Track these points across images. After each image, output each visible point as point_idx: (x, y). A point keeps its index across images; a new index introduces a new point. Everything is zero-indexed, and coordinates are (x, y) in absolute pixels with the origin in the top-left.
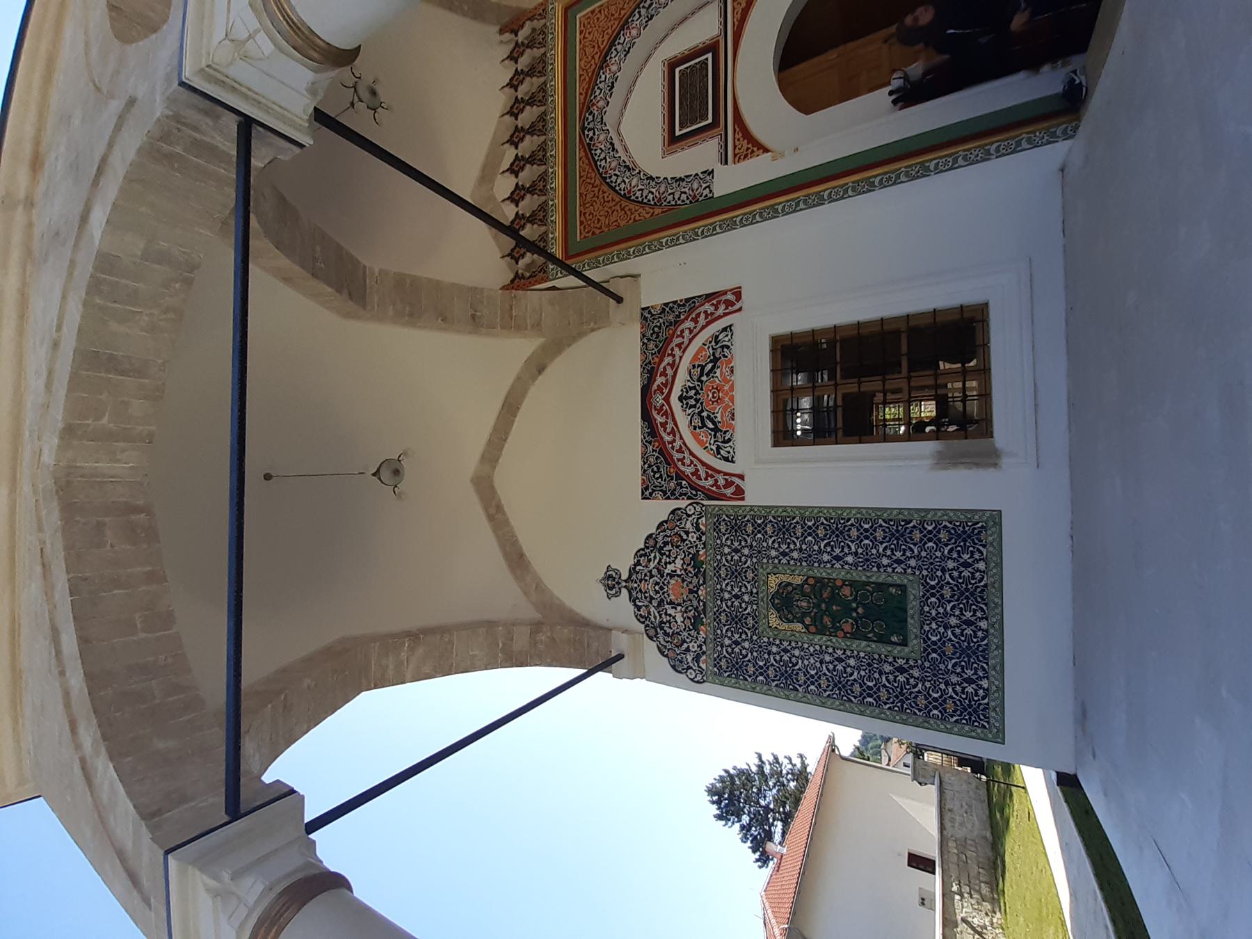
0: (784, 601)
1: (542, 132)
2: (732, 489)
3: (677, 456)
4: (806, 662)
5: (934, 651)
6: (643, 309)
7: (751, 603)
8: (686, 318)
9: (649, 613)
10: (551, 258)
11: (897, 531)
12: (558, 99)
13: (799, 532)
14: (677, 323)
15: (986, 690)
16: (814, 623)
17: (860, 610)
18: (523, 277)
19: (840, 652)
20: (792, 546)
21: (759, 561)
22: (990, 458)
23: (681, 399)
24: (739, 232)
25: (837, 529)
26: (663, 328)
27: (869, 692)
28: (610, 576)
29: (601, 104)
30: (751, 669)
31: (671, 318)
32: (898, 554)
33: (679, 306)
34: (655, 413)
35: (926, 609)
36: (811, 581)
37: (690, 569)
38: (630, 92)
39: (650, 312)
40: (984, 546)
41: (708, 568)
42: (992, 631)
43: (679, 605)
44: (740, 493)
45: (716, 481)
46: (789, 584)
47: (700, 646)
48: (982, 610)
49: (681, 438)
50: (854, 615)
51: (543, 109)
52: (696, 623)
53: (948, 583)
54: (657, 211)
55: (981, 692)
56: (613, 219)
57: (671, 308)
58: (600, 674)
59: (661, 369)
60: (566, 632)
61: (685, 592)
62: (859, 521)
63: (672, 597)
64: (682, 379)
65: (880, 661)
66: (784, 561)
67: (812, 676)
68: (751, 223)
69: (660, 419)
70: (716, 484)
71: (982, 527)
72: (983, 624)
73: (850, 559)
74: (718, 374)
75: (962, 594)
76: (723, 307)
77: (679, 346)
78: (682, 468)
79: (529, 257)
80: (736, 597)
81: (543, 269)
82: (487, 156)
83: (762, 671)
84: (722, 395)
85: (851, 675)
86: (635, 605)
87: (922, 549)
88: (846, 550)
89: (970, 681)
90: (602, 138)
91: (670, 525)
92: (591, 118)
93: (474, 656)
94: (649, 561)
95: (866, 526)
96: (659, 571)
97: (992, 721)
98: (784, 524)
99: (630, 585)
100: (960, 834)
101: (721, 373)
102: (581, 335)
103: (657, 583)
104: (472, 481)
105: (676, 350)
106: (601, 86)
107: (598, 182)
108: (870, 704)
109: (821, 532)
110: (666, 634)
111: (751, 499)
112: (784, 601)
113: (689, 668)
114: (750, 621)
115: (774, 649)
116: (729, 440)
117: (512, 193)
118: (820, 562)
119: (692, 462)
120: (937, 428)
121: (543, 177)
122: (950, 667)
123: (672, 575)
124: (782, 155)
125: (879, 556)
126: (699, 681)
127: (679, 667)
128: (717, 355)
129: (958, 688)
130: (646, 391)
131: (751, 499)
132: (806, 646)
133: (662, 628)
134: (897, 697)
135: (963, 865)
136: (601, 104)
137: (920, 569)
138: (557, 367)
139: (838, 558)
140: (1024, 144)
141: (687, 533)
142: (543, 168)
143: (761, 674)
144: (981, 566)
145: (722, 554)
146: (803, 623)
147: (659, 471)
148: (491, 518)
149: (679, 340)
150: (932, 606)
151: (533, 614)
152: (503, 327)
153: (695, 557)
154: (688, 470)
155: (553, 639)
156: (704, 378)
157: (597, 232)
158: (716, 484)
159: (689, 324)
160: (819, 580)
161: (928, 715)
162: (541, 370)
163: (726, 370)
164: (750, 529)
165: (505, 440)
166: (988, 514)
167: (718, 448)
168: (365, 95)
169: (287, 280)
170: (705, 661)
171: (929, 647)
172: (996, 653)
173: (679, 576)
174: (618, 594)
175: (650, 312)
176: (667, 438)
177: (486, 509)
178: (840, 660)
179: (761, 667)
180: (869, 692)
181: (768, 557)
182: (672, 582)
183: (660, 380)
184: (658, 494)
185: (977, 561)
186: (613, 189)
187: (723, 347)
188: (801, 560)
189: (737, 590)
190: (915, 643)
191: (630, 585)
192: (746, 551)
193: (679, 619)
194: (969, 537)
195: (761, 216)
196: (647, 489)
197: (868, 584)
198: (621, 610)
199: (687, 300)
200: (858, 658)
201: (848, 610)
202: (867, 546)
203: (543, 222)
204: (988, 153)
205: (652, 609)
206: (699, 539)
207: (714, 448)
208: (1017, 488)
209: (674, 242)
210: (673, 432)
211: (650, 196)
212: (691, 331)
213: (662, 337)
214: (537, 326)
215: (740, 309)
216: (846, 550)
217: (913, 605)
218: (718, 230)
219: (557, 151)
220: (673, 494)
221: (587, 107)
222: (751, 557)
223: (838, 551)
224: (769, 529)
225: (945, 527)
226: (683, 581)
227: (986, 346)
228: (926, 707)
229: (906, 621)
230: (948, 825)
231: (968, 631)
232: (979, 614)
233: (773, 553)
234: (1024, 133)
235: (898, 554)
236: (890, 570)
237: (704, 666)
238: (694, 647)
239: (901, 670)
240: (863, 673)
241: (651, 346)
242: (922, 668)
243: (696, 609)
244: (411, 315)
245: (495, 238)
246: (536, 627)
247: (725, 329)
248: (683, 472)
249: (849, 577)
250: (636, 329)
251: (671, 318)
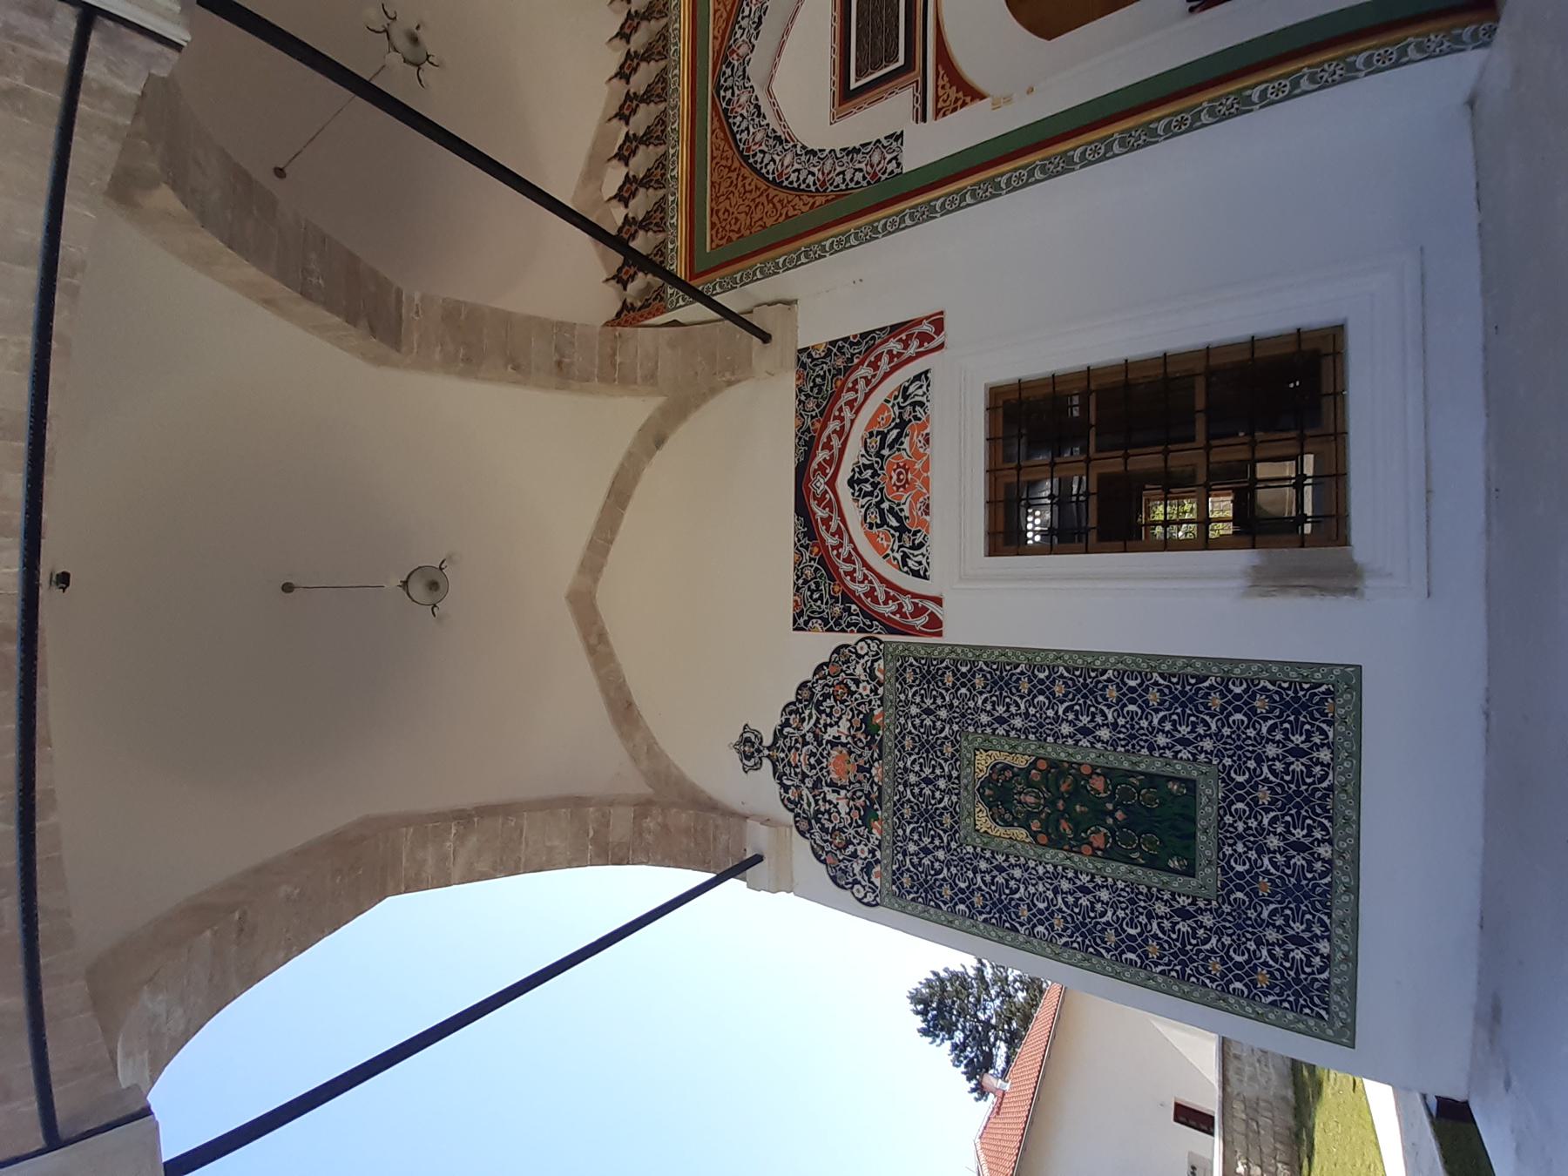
0: (1000, 792)
1: (662, 98)
2: (924, 619)
3: (845, 568)
4: (1032, 890)
5: (1240, 888)
6: (800, 351)
7: (950, 792)
8: (861, 363)
9: (801, 797)
10: (671, 278)
11: (1184, 693)
12: (684, 47)
13: (1025, 687)
14: (849, 369)
15: (1327, 959)
16: (1045, 825)
17: (1119, 815)
18: (633, 308)
19: (1085, 878)
20: (1013, 709)
21: (962, 730)
22: (1345, 580)
23: (851, 483)
24: (940, 222)
25: (1085, 685)
26: (828, 377)
27: (1131, 944)
28: (748, 740)
29: (742, 51)
30: (947, 892)
31: (840, 363)
32: (1184, 730)
33: (852, 344)
34: (814, 504)
35: (1228, 819)
36: (1042, 765)
37: (860, 735)
38: (787, 32)
39: (810, 356)
40: (1330, 723)
41: (887, 736)
42: (1339, 863)
43: (843, 787)
44: (935, 624)
45: (901, 606)
46: (1007, 767)
47: (872, 852)
48: (1324, 828)
49: (851, 541)
50: (1110, 821)
51: (662, 64)
52: (867, 816)
53: (1266, 780)
54: (820, 200)
55: (1317, 960)
56: (756, 217)
57: (840, 349)
58: (732, 880)
59: (824, 439)
60: (684, 818)
61: (852, 768)
62: (1121, 674)
63: (834, 776)
64: (854, 453)
65: (1149, 896)
66: (1001, 731)
67: (1041, 912)
68: (959, 208)
69: (820, 513)
71: (1328, 692)
72: (1324, 851)
73: (1104, 733)
74: (906, 446)
75: (1290, 799)
76: (916, 343)
77: (850, 403)
78: (852, 586)
79: (641, 280)
80: (927, 781)
81: (659, 295)
82: (594, 144)
83: (964, 896)
84: (913, 477)
85: (1103, 914)
86: (782, 784)
87: (1224, 722)
88: (1099, 719)
89: (1298, 941)
90: (743, 99)
91: (832, 669)
92: (729, 71)
93: (551, 849)
94: (803, 720)
95: (1132, 683)
96: (816, 737)
97: (1334, 1007)
98: (1002, 674)
99: (774, 753)
100: (1249, 1091)
101: (911, 444)
102: (714, 391)
103: (813, 754)
104: (567, 597)
105: (847, 410)
106: (744, 23)
107: (736, 164)
108: (1131, 963)
109: (1059, 689)
110: (824, 829)
111: (954, 633)
112: (1000, 792)
113: (856, 882)
114: (947, 820)
115: (983, 865)
116: (921, 545)
117: (621, 189)
118: (1056, 736)
119: (866, 577)
120: (1252, 527)
121: (662, 163)
122: (1265, 915)
123: (834, 743)
124: (1008, 100)
125: (1152, 731)
126: (870, 903)
127: (841, 879)
128: (906, 417)
129: (1278, 951)
130: (802, 472)
131: (954, 633)
132: (1032, 864)
133: (818, 821)
134: (1175, 955)
135: (1252, 1137)
136: (742, 51)
137: (1220, 755)
138: (681, 439)
139: (1085, 731)
140: (1412, 53)
141: (857, 682)
142: (661, 149)
143: (962, 901)
144: (1325, 755)
145: (907, 716)
146: (1028, 828)
147: (818, 590)
148: (591, 651)
149: (851, 395)
150: (1239, 815)
151: (639, 787)
152: (602, 379)
153: (867, 718)
154: (860, 589)
155: (665, 827)
156: (886, 452)
157: (734, 236)
159: (864, 371)
160: (1054, 764)
161: (1225, 989)
162: (659, 442)
163: (918, 439)
164: (949, 679)
165: (611, 542)
166: (1337, 672)
167: (905, 556)
168: (401, 42)
169: (268, 303)
170: (879, 875)
171: (1232, 881)
172: (1345, 898)
173: (844, 745)
174: (757, 767)
175: (810, 356)
176: (831, 541)
177: (585, 637)
178: (1085, 890)
179: (962, 891)
180: (1131, 944)
181: (977, 724)
182: (834, 753)
183: (822, 455)
184: (817, 623)
185: (1318, 747)
186: (758, 172)
187: (914, 404)
188: (1026, 732)
189: (928, 771)
190: (1208, 875)
191: (774, 753)
192: (943, 713)
193: (843, 808)
194: (1305, 706)
195: (973, 196)
196: (800, 614)
197: (1133, 774)
198: (759, 790)
199: (864, 335)
200: (1113, 889)
201: (1099, 815)
202: (1132, 715)
203: (661, 227)
204: (1352, 67)
205: (805, 792)
206: (874, 691)
207: (898, 556)
209: (842, 245)
210: (839, 533)
211: (811, 179)
212: (868, 382)
213: (828, 389)
214: (651, 378)
215: (941, 346)
216: (1099, 719)
217: (1206, 813)
218: (908, 222)
219: (681, 124)
220: (837, 624)
221: (723, 57)
222: (950, 722)
223: (1085, 719)
224: (979, 682)
225: (1264, 689)
226: (850, 752)
227: (1338, 396)
228: (1223, 976)
229: (1194, 836)
230: (1231, 1074)
231: (1299, 861)
232: (1318, 834)
233: (984, 718)
234: (1411, 37)
235: (1184, 730)
236: (1169, 754)
237: (877, 882)
238: (863, 852)
239: (1184, 914)
240: (1121, 914)
241: (811, 405)
242: (1218, 913)
243: (868, 796)
244: (467, 360)
245: (603, 258)
246: (643, 807)
247: (917, 378)
248: (853, 592)
249: (1102, 761)
250: (789, 381)
251: (840, 363)
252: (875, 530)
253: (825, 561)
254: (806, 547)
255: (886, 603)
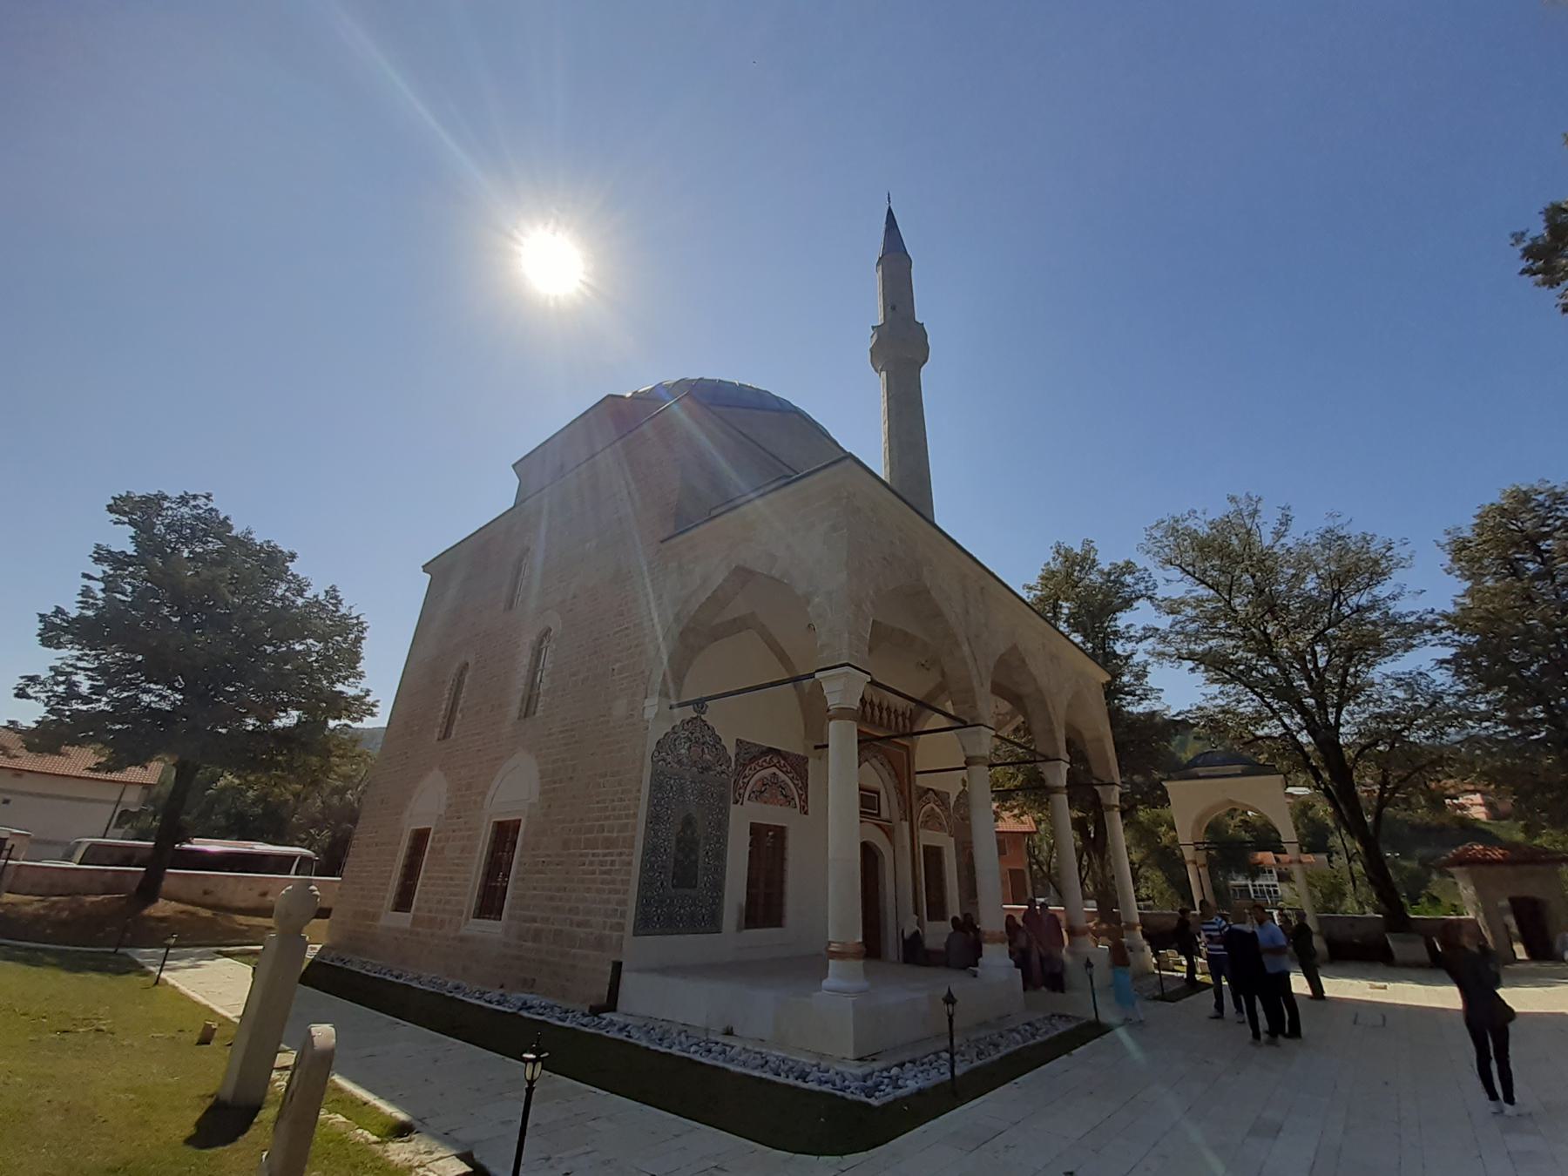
22: (739, 929)
44: (736, 802)
98: (722, 825)
112: (688, 822)
130: (777, 752)
131: (733, 808)
208: (732, 937)
217: (687, 891)
253: (754, 759)
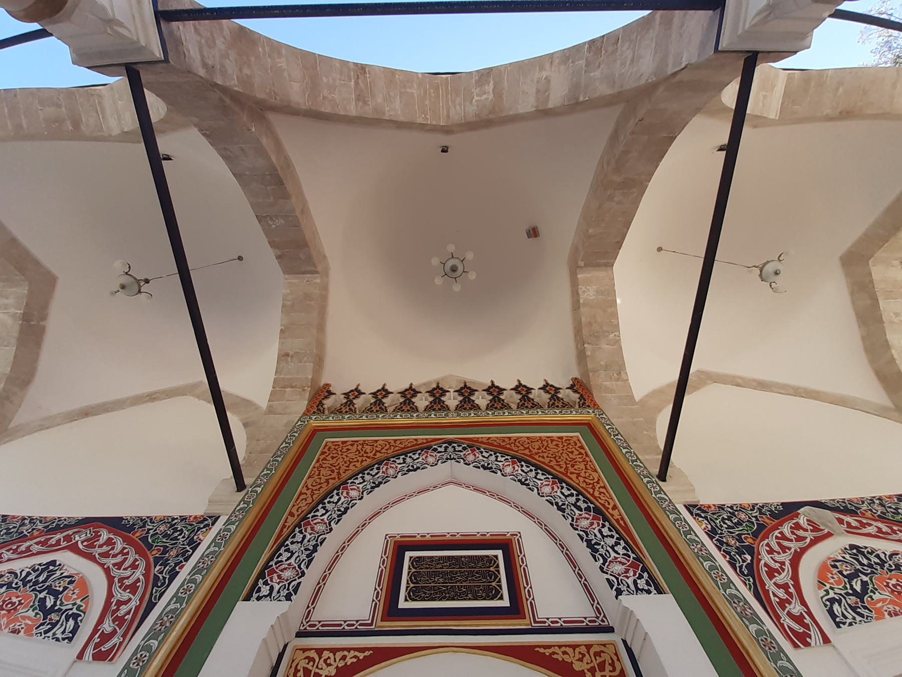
23: (852, 547)
45: (790, 603)
64: (884, 547)
70: (783, 603)
119: (783, 563)
154: (766, 558)
158: (783, 603)
176: (786, 529)
252: (835, 571)
254: (761, 513)
255: (778, 586)
